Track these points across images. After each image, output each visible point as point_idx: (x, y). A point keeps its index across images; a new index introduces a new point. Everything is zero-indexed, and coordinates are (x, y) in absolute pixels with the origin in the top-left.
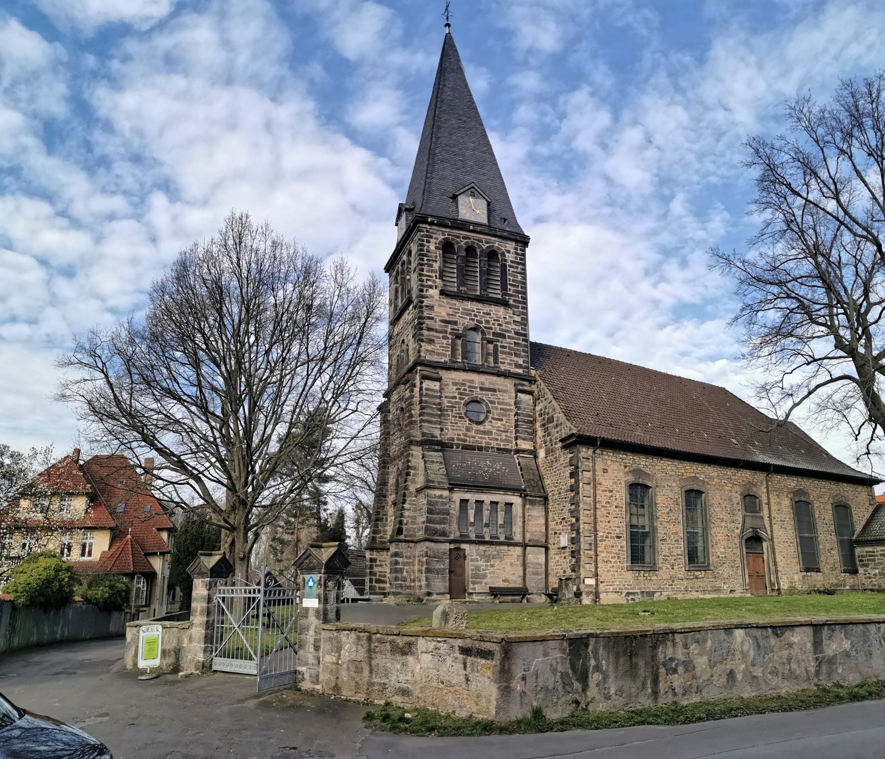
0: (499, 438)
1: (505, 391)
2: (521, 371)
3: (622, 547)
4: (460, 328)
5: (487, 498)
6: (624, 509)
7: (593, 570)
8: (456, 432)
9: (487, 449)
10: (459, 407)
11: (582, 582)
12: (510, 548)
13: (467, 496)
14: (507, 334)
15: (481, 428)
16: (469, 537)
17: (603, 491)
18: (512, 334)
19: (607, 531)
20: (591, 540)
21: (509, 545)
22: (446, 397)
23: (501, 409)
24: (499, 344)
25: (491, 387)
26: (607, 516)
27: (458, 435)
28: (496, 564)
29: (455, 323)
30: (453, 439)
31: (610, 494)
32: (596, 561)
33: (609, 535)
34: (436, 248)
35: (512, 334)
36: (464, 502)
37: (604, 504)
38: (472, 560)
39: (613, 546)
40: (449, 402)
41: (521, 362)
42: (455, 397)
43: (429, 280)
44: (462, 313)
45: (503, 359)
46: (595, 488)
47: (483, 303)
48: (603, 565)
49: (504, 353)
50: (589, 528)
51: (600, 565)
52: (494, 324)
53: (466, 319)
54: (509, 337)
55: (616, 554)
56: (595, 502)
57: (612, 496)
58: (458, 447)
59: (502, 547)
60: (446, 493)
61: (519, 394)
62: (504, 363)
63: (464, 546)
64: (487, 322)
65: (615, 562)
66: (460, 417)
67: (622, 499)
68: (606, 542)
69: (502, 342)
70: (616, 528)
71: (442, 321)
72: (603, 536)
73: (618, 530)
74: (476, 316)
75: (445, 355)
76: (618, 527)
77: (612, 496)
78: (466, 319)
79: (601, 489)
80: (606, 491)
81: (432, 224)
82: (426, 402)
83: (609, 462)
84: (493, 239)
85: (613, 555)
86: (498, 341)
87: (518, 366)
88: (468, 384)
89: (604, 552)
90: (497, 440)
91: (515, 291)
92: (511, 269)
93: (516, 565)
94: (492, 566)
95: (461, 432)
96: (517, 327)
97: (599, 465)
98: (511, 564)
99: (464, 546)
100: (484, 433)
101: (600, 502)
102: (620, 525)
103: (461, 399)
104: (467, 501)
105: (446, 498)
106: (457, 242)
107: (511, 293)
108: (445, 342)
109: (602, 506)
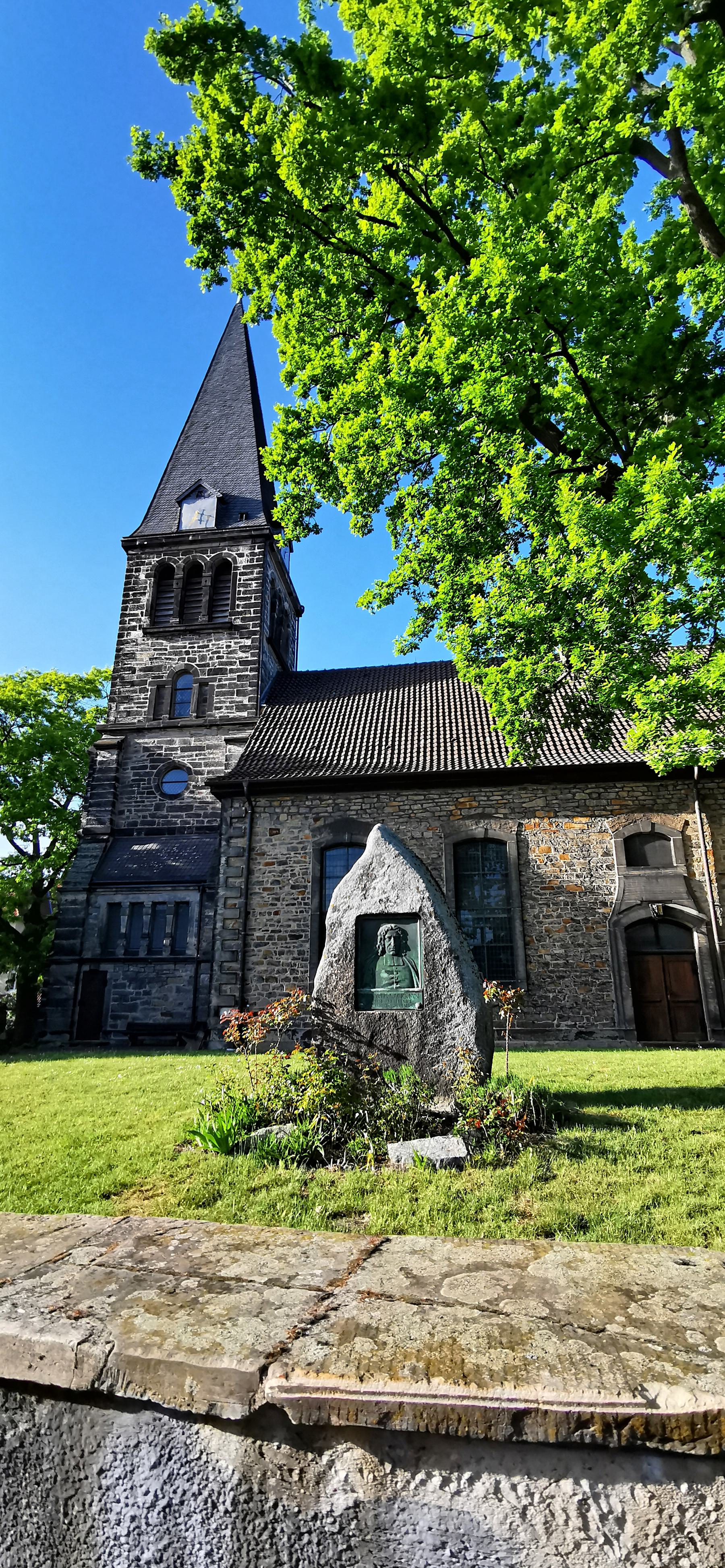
0: (202, 812)
1: (216, 747)
2: (245, 714)
3: (300, 953)
4: (165, 675)
5: (146, 898)
6: (309, 890)
7: (237, 994)
8: (140, 814)
9: (181, 830)
10: (149, 780)
11: (212, 1012)
12: (178, 967)
13: (118, 898)
14: (228, 668)
15: (177, 803)
16: (113, 953)
17: (267, 864)
18: (237, 666)
19: (270, 929)
20: (238, 945)
21: (176, 961)
22: (133, 768)
23: (209, 772)
24: (216, 684)
25: (198, 744)
26: (272, 905)
27: (144, 817)
28: (154, 991)
29: (159, 668)
30: (135, 824)
31: (281, 868)
32: (244, 981)
33: (276, 935)
34: (147, 576)
35: (237, 666)
36: (114, 908)
37: (269, 886)
38: (115, 986)
39: (282, 953)
40: (135, 775)
41: (246, 701)
42: (145, 767)
43: (132, 620)
44: (170, 654)
45: (220, 702)
46: (249, 859)
47: (199, 634)
48: (260, 985)
49: (224, 694)
50: (236, 926)
51: (253, 984)
52: (211, 658)
53: (173, 660)
54: (232, 671)
55: (288, 965)
56: (248, 882)
57: (285, 871)
58: (139, 833)
59: (165, 967)
60: (82, 897)
61: (229, 746)
62: (221, 708)
63: (104, 967)
64: (203, 658)
65: (287, 979)
66: (148, 793)
67: (305, 873)
68: (270, 947)
69: (220, 680)
70: (291, 923)
71: (140, 670)
72: (262, 938)
73: (294, 925)
74: (187, 653)
75: (138, 713)
76: (294, 920)
77: (285, 871)
78: (173, 660)
79: (263, 861)
80: (273, 864)
81: (142, 547)
82: (98, 779)
83: (283, 817)
84: (222, 544)
85: (280, 968)
86: (214, 680)
87: (241, 707)
88: (164, 746)
89: (262, 963)
90: (199, 816)
91: (245, 606)
92: (243, 578)
93: (187, 991)
94: (147, 993)
95: (147, 813)
96: (244, 655)
97: (263, 825)
98: (178, 990)
99: (104, 967)
100: (181, 809)
101: (261, 883)
102: (300, 916)
103: (153, 767)
104: (119, 905)
105: (81, 903)
106: (176, 562)
107: (240, 609)
108: (143, 696)
109: (264, 889)
